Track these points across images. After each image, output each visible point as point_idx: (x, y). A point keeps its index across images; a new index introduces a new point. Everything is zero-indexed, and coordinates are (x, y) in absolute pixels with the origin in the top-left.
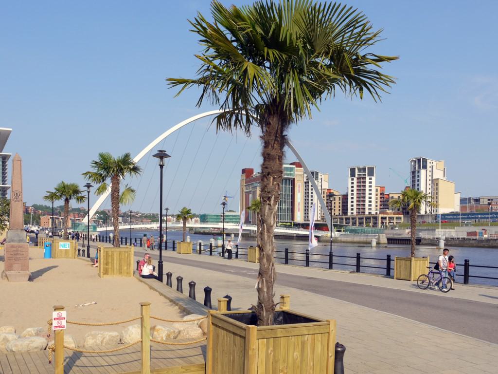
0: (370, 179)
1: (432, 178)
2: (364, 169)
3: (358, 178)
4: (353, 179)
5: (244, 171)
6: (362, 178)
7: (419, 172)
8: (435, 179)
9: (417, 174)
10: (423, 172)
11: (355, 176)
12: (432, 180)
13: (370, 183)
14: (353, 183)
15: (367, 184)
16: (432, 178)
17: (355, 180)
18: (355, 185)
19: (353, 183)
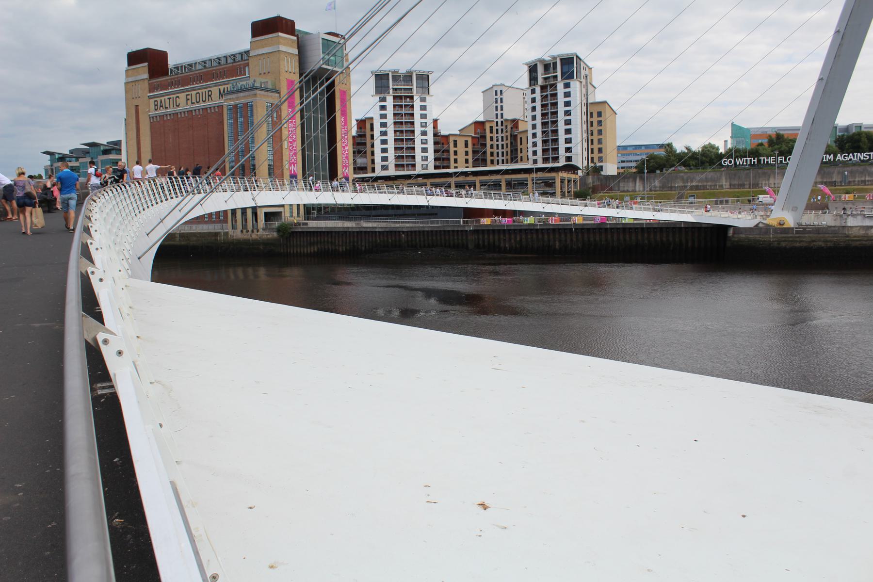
0: (423, 100)
1: (587, 100)
2: (408, 77)
3: (395, 97)
4: (383, 100)
5: (134, 58)
6: (406, 97)
7: (567, 86)
8: (591, 104)
9: (561, 89)
10: (575, 85)
11: (389, 93)
12: (587, 104)
13: (423, 108)
14: (383, 108)
15: (417, 112)
16: (587, 100)
17: (390, 102)
18: (390, 111)
19: (383, 108)
